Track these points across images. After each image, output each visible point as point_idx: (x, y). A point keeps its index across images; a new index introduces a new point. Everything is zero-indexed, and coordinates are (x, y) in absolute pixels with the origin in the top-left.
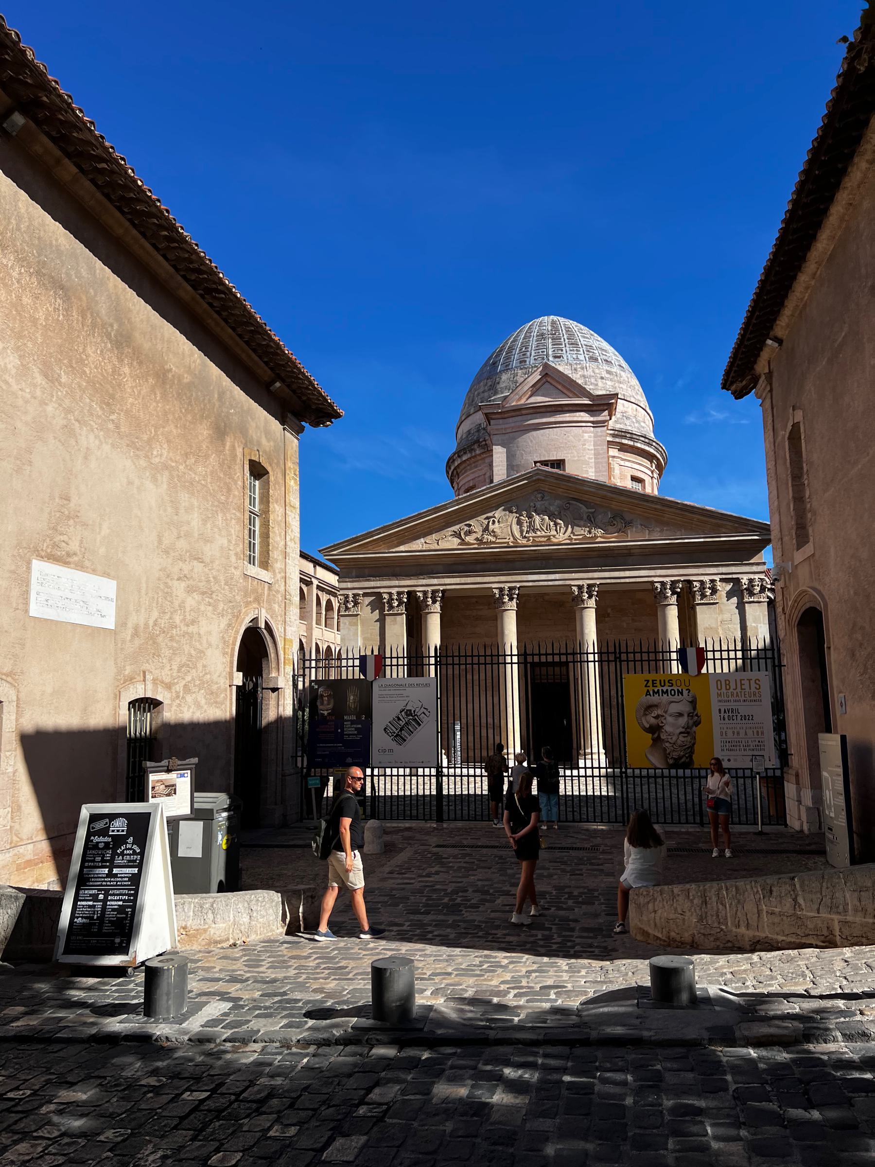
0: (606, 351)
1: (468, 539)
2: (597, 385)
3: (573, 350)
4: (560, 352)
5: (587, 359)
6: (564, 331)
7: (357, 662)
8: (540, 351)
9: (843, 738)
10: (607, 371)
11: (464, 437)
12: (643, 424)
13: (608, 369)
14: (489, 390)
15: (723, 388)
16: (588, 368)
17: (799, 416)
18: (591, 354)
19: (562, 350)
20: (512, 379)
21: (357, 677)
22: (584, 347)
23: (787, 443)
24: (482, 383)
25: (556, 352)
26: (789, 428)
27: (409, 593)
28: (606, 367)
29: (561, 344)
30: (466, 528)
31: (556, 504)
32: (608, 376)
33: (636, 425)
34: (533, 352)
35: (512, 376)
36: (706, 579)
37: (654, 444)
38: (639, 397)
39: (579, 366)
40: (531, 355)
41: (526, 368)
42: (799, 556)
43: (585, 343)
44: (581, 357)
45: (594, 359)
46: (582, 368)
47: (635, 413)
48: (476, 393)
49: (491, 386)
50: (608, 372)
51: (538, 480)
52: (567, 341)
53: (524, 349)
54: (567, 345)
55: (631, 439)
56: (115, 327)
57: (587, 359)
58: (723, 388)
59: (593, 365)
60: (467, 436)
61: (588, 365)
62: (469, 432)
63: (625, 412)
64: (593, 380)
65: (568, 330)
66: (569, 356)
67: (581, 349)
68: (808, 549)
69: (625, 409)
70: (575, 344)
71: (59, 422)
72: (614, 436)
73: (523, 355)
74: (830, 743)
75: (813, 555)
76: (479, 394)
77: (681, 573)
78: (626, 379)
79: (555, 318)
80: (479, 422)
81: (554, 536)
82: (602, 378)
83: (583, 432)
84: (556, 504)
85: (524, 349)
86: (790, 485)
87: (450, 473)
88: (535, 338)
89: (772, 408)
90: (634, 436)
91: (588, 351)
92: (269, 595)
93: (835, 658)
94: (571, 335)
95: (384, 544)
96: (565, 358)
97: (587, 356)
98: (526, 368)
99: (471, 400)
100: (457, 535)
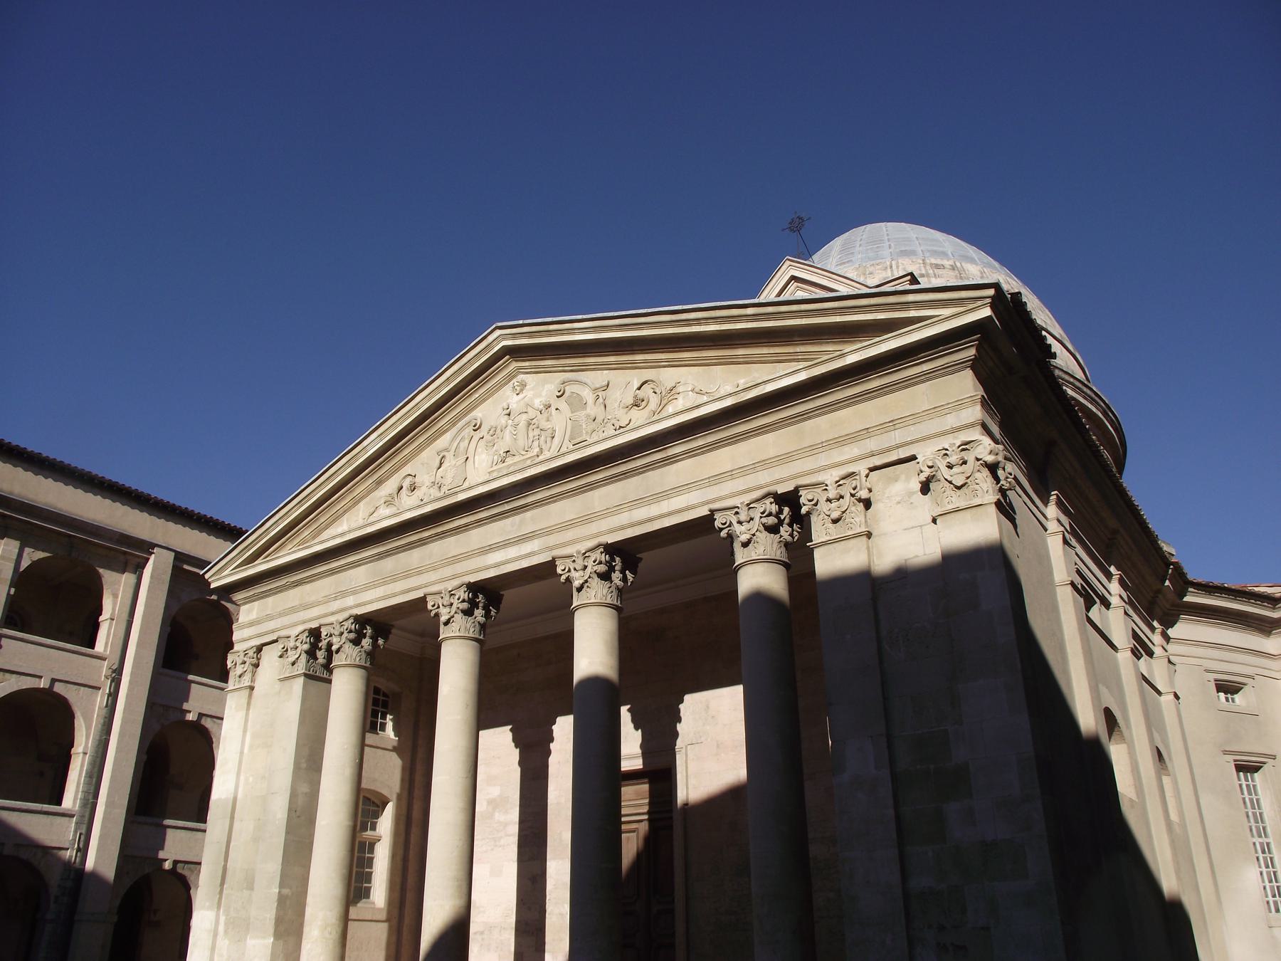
31: (544, 393)
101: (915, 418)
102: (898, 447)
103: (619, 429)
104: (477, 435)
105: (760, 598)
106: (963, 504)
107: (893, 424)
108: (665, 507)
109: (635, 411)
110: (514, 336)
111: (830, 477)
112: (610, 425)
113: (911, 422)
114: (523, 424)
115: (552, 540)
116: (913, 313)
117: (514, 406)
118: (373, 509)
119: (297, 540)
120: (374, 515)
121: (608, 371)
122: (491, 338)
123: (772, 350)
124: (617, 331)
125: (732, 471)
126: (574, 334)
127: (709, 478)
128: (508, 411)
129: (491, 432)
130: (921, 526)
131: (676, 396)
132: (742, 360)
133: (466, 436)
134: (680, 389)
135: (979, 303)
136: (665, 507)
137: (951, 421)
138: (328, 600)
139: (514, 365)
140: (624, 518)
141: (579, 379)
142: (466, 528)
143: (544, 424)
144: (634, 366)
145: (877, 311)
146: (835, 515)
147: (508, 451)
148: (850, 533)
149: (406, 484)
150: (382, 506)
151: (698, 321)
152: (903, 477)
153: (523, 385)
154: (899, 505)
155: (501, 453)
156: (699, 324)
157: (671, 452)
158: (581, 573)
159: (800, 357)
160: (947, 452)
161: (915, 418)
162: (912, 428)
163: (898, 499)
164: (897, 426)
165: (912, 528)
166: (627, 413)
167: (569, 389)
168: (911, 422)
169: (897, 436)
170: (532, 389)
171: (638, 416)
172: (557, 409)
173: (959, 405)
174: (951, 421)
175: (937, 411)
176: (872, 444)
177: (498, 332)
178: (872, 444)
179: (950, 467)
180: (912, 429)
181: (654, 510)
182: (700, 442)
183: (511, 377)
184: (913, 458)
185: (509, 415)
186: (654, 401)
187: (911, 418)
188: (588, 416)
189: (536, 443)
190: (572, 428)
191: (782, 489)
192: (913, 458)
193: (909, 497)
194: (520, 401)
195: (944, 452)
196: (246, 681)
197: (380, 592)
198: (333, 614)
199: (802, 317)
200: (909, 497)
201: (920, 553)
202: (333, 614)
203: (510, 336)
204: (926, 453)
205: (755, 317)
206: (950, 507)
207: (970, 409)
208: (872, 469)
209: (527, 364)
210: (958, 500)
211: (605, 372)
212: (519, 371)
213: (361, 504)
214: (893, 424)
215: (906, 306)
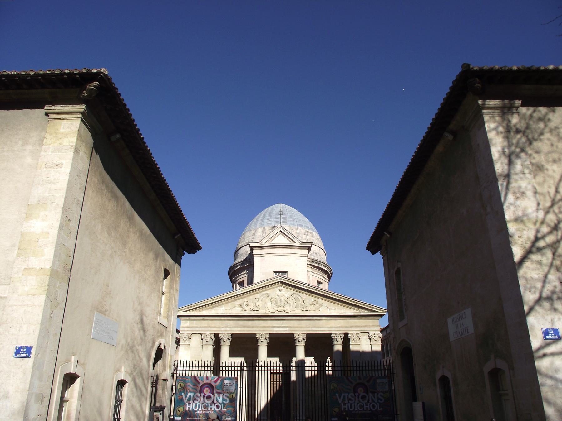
1: (246, 308)
2: (302, 237)
9: (423, 403)
12: (322, 257)
17: (399, 265)
23: (394, 275)
26: (396, 269)
27: (215, 334)
30: (246, 303)
33: (319, 257)
36: (355, 333)
37: (327, 266)
38: (321, 244)
39: (294, 228)
42: (401, 324)
47: (319, 251)
55: (317, 263)
56: (130, 212)
58: (367, 249)
63: (315, 251)
64: (300, 235)
68: (405, 322)
69: (315, 250)
71: (110, 252)
72: (310, 261)
74: (418, 406)
75: (407, 324)
77: (344, 330)
81: (287, 309)
84: (288, 294)
86: (396, 293)
87: (231, 274)
89: (388, 260)
90: (319, 262)
92: (165, 333)
93: (417, 369)
100: (240, 306)
101: (370, 326)
105: (338, 351)
106: (376, 343)
108: (320, 329)
110: (284, 280)
115: (292, 329)
116: (373, 309)
119: (205, 308)
122: (278, 278)
123: (344, 305)
136: (320, 329)
137: (375, 328)
138: (219, 327)
139: (280, 284)
140: (310, 329)
141: (299, 294)
142: (267, 320)
144: (312, 296)
148: (357, 344)
149: (246, 303)
151: (332, 295)
157: (322, 318)
161: (370, 326)
169: (366, 328)
170: (284, 291)
171: (313, 308)
173: (377, 326)
174: (375, 328)
175: (373, 326)
176: (362, 329)
177: (280, 278)
178: (362, 329)
179: (375, 337)
181: (317, 329)
182: (329, 318)
183: (278, 286)
196: (187, 343)
197: (239, 329)
198: (222, 331)
201: (368, 349)
202: (222, 331)
205: (344, 299)
209: (284, 285)
212: (281, 286)
213: (229, 304)
214: (366, 326)
215: (373, 308)
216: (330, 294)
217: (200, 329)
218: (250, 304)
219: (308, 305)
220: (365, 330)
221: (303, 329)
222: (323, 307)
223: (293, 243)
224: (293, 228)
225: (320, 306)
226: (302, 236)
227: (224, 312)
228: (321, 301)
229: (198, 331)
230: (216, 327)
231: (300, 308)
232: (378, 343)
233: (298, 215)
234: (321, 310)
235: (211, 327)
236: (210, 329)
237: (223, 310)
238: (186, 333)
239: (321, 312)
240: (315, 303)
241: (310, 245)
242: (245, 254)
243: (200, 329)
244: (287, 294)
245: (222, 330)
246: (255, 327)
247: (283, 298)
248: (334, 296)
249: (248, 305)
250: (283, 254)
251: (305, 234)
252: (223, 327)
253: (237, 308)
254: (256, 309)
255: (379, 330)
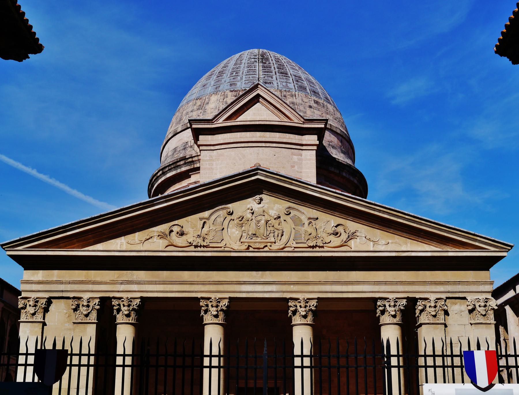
0: (313, 83)
2: (305, 112)
3: (283, 78)
4: (270, 79)
5: (296, 88)
6: (274, 62)
7: (31, 360)
8: (251, 76)
10: (314, 101)
11: (169, 154)
13: (316, 99)
14: (198, 109)
15: (496, 52)
16: (297, 96)
18: (300, 84)
19: (272, 78)
20: (221, 100)
21: (29, 379)
22: (293, 77)
24: (191, 103)
25: (266, 78)
28: (314, 98)
29: (271, 72)
31: (275, 208)
32: (315, 105)
34: (244, 77)
35: (222, 97)
39: (288, 94)
40: (242, 79)
41: (236, 91)
43: (294, 73)
44: (291, 86)
45: (302, 88)
46: (292, 96)
48: (184, 112)
49: (200, 105)
50: (316, 102)
51: (258, 179)
52: (277, 70)
53: (234, 74)
54: (277, 73)
57: (296, 88)
59: (302, 94)
60: (173, 154)
61: (297, 93)
62: (175, 150)
64: (302, 108)
65: (277, 60)
66: (279, 83)
67: (291, 79)
70: (285, 74)
73: (234, 79)
76: (187, 113)
77: (407, 290)
78: (332, 111)
79: (265, 51)
80: (186, 140)
82: (310, 107)
83: (293, 154)
85: (234, 74)
88: (246, 65)
91: (297, 81)
94: (281, 67)
95: (78, 242)
96: (276, 85)
97: (296, 86)
98: (236, 91)
99: (178, 119)
101: (468, 283)
102: (459, 292)
103: (325, 244)
104: (229, 218)
106: (484, 322)
107: (459, 283)
109: (332, 236)
110: (267, 176)
111: (433, 297)
112: (320, 240)
113: (466, 284)
114: (263, 222)
116: (477, 244)
117: (257, 210)
118: (148, 237)
120: (149, 240)
121: (316, 211)
124: (335, 199)
125: (386, 282)
126: (307, 190)
127: (375, 282)
128: (253, 211)
129: (240, 219)
130: (465, 325)
131: (356, 237)
132: (391, 232)
133: (222, 215)
134: (358, 234)
135: (504, 250)
140: (328, 288)
141: (299, 209)
143: (276, 226)
145: (463, 237)
146: (434, 313)
147: (255, 234)
149: (176, 229)
150: (156, 237)
151: (380, 211)
152: (459, 304)
153: (261, 200)
154: (456, 314)
155: (250, 233)
156: (380, 212)
158: (304, 309)
159: (420, 240)
160: (480, 300)
161: (468, 283)
162: (466, 286)
163: (456, 312)
164: (460, 284)
165: (461, 325)
166: (327, 236)
167: (293, 213)
168: (466, 284)
170: (267, 203)
171: (336, 241)
172: (285, 220)
180: (466, 287)
184: (464, 298)
185: (253, 213)
186: (344, 237)
187: (466, 282)
188: (306, 231)
189: (272, 235)
190: (295, 234)
191: (411, 295)
192: (464, 298)
193: (461, 312)
194: (260, 208)
195: (479, 300)
196: (39, 317)
199: (430, 228)
200: (461, 312)
202: (118, 292)
203: (266, 176)
204: (469, 297)
206: (478, 321)
207: (489, 286)
208: (447, 298)
210: (482, 320)
211: (314, 210)
215: (476, 240)
216: (374, 209)
217: (69, 287)
218: (185, 229)
219: (324, 235)
220: (458, 290)
221: (310, 288)
222: (358, 240)
223: (286, 120)
224: (285, 93)
225: (352, 236)
226: (304, 110)
227: (124, 249)
228: (352, 225)
229: (62, 291)
230: (106, 283)
231: (303, 241)
232: (488, 322)
233: (296, 70)
234: (353, 246)
235: (94, 283)
236: (90, 287)
237: (121, 244)
238: (34, 295)
239: (353, 250)
240: (340, 229)
241: (323, 126)
242: (183, 148)
243: (69, 287)
244: (273, 209)
245: (121, 289)
246: (198, 284)
247: (263, 218)
248: (384, 212)
249: (182, 234)
250: (263, 145)
251: (310, 107)
252: (121, 283)
253: (155, 239)
254: (200, 241)
255: (489, 292)
